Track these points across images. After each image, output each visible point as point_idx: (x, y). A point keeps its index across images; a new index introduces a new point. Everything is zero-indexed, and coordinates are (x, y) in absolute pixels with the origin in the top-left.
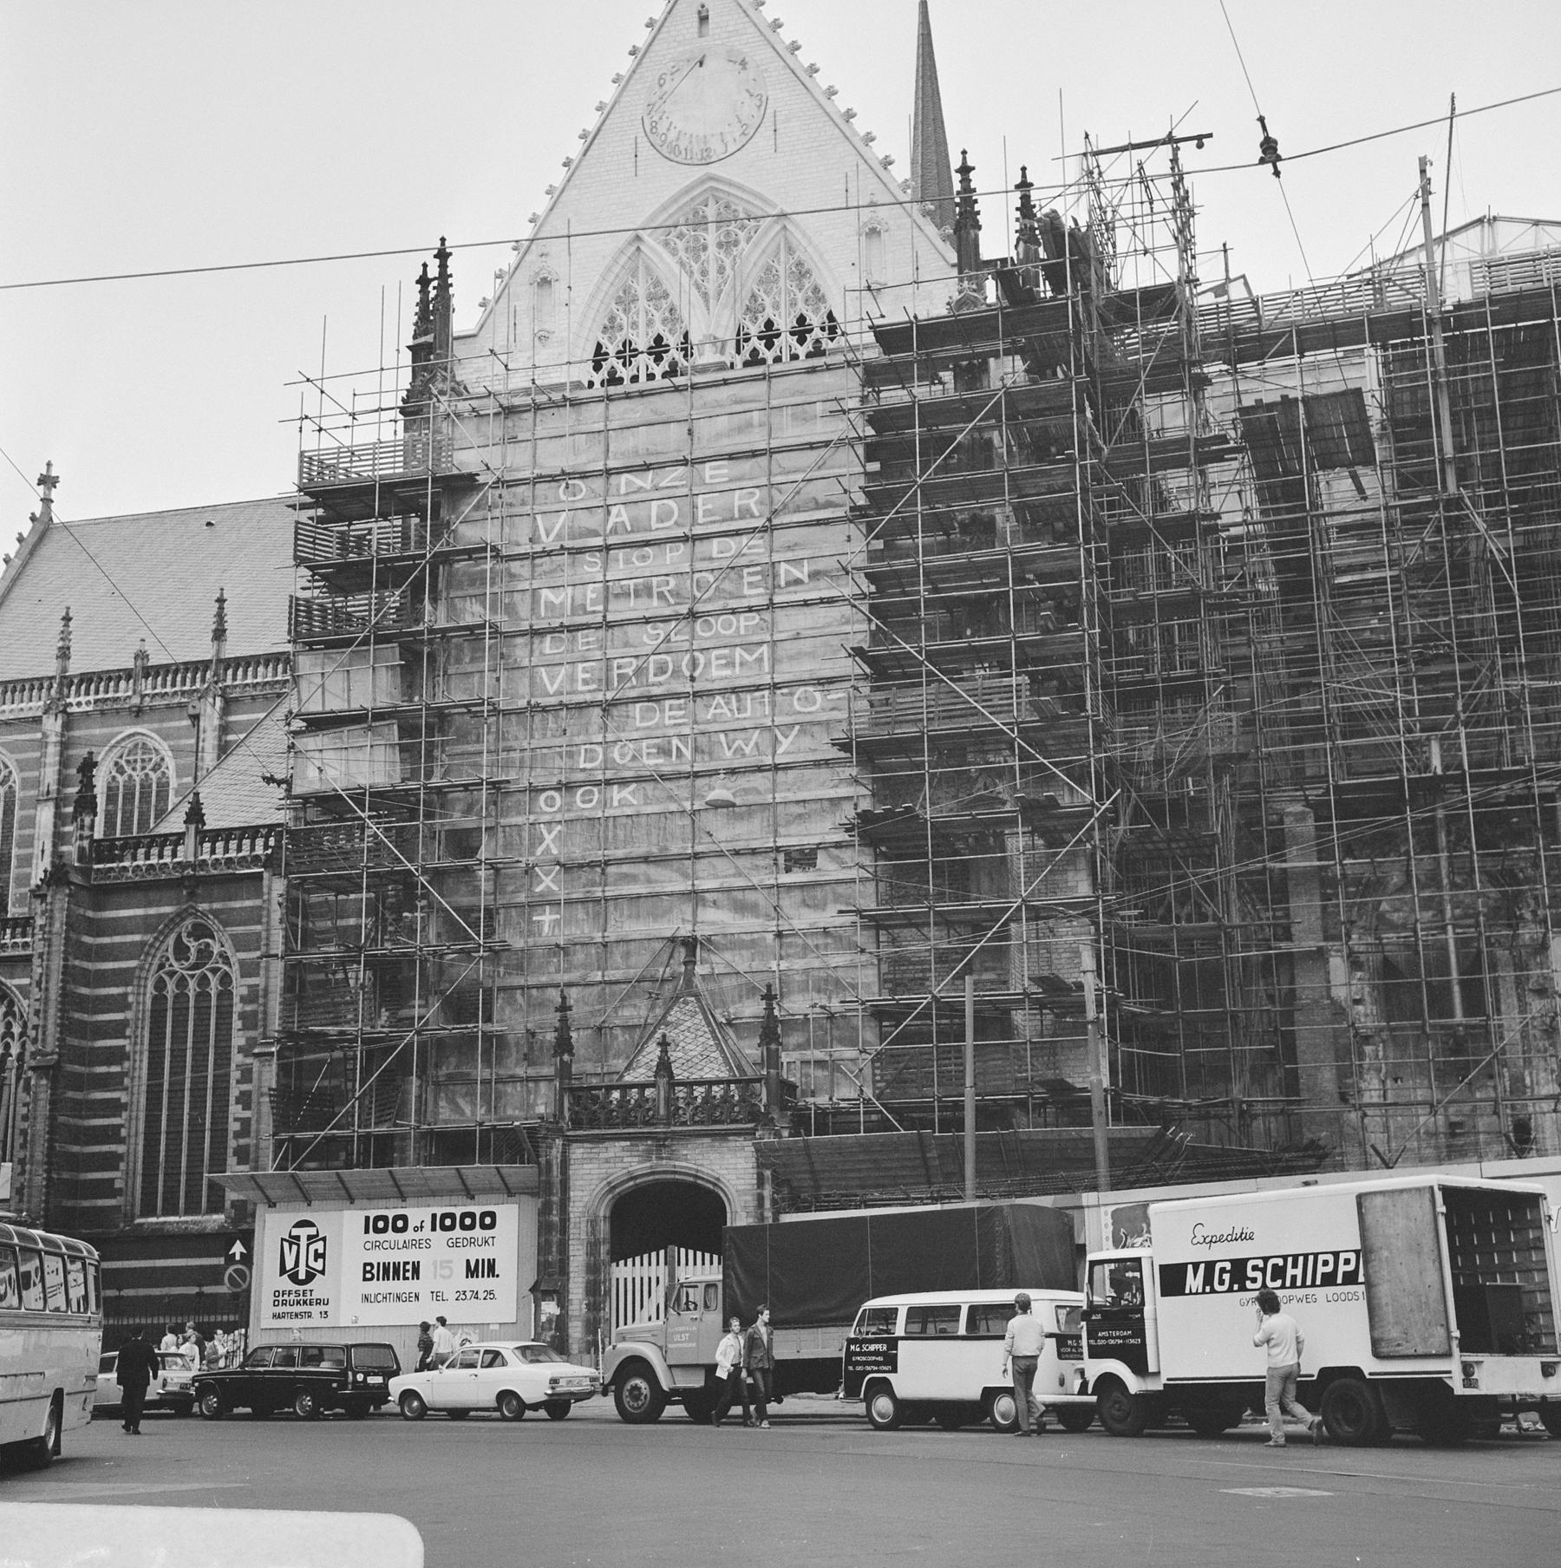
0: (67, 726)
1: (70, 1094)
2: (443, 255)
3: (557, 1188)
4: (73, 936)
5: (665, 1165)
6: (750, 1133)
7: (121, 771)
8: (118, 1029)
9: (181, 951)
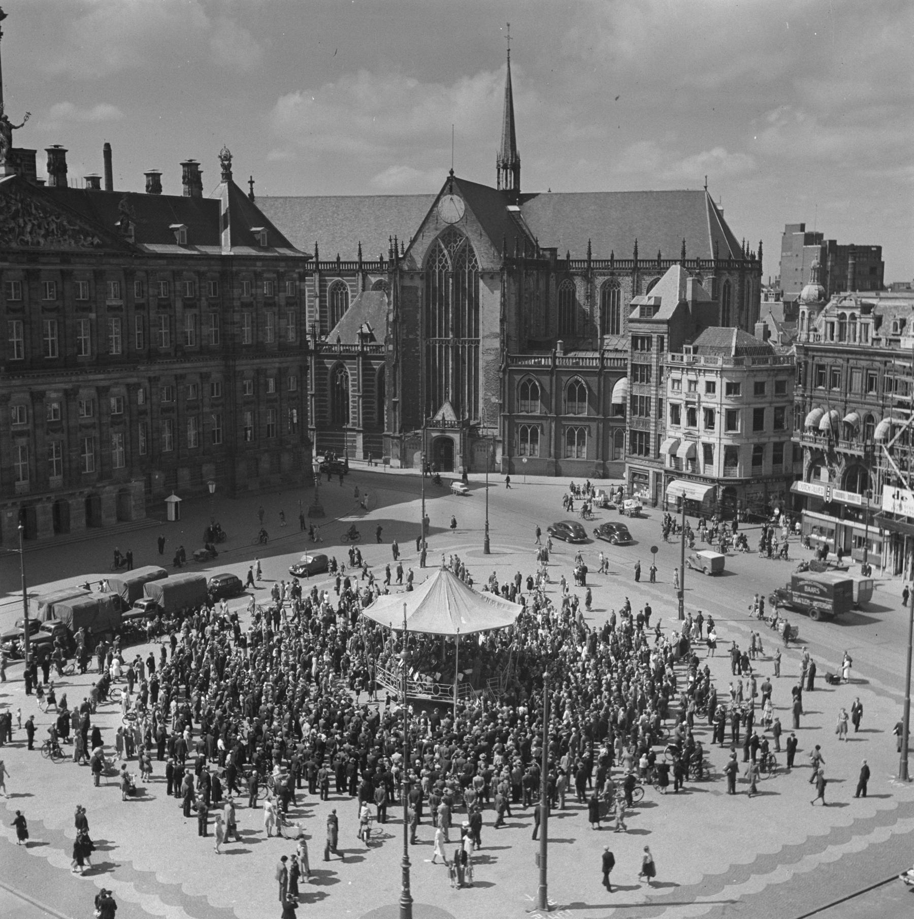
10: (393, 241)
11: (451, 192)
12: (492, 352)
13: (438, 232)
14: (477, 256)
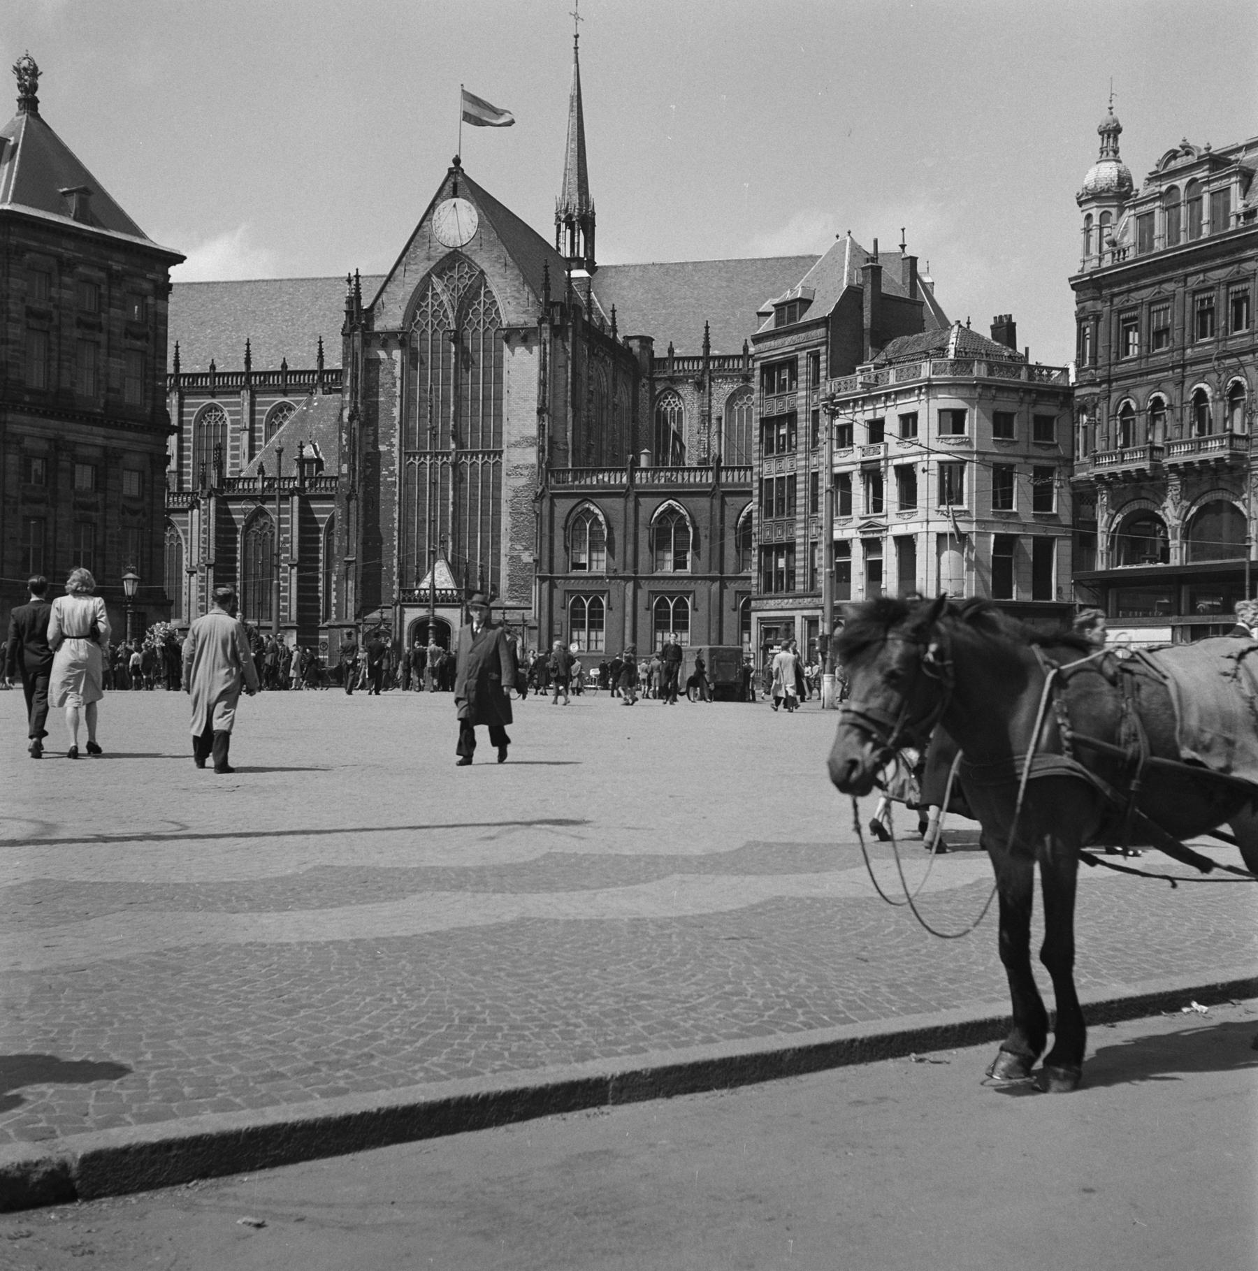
10: (354, 282)
11: (455, 194)
12: (525, 472)
13: (433, 264)
14: (500, 304)
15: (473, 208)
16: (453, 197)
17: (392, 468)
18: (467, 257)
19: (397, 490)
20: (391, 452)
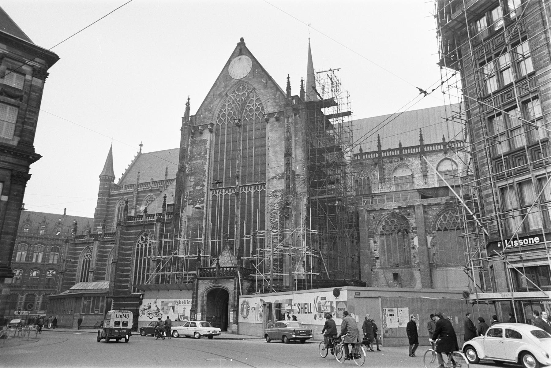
0: (138, 194)
1: (120, 268)
2: (189, 99)
3: (196, 290)
4: (122, 236)
5: (217, 285)
6: (233, 278)
7: (148, 202)
8: (129, 255)
9: (142, 239)
12: (279, 194)
15: (250, 59)
16: (239, 56)
17: (203, 199)
18: (246, 82)
19: (205, 211)
20: (202, 189)
